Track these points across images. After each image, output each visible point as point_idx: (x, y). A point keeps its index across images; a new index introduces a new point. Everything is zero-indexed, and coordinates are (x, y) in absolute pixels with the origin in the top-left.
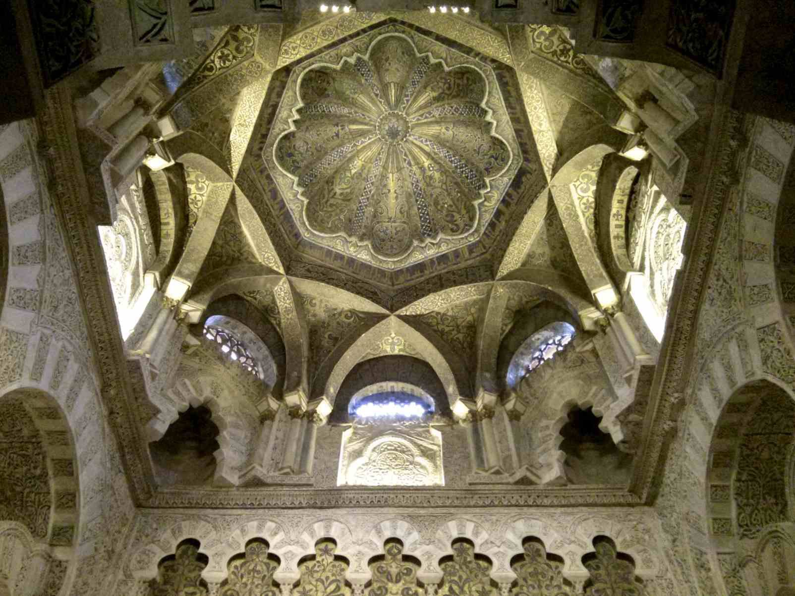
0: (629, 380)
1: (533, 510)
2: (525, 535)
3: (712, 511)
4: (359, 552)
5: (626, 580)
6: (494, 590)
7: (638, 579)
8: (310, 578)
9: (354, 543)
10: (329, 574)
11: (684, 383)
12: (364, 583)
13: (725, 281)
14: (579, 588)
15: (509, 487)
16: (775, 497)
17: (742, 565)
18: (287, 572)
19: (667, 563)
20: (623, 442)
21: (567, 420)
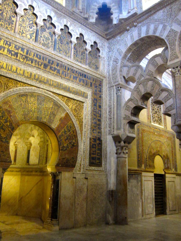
0: (129, 12)
1: (84, 27)
2: (81, 33)
3: (126, 52)
4: (41, 16)
5: (96, 55)
6: (70, 43)
7: (99, 56)
8: (25, 16)
9: (39, 11)
10: (31, 18)
11: (140, 22)
12: (41, 25)
13: (172, 10)
14: (88, 52)
15: (82, 18)
16: (137, 57)
17: (124, 66)
18: (20, 11)
19: (106, 55)
20: (115, 24)
21: (101, 7)
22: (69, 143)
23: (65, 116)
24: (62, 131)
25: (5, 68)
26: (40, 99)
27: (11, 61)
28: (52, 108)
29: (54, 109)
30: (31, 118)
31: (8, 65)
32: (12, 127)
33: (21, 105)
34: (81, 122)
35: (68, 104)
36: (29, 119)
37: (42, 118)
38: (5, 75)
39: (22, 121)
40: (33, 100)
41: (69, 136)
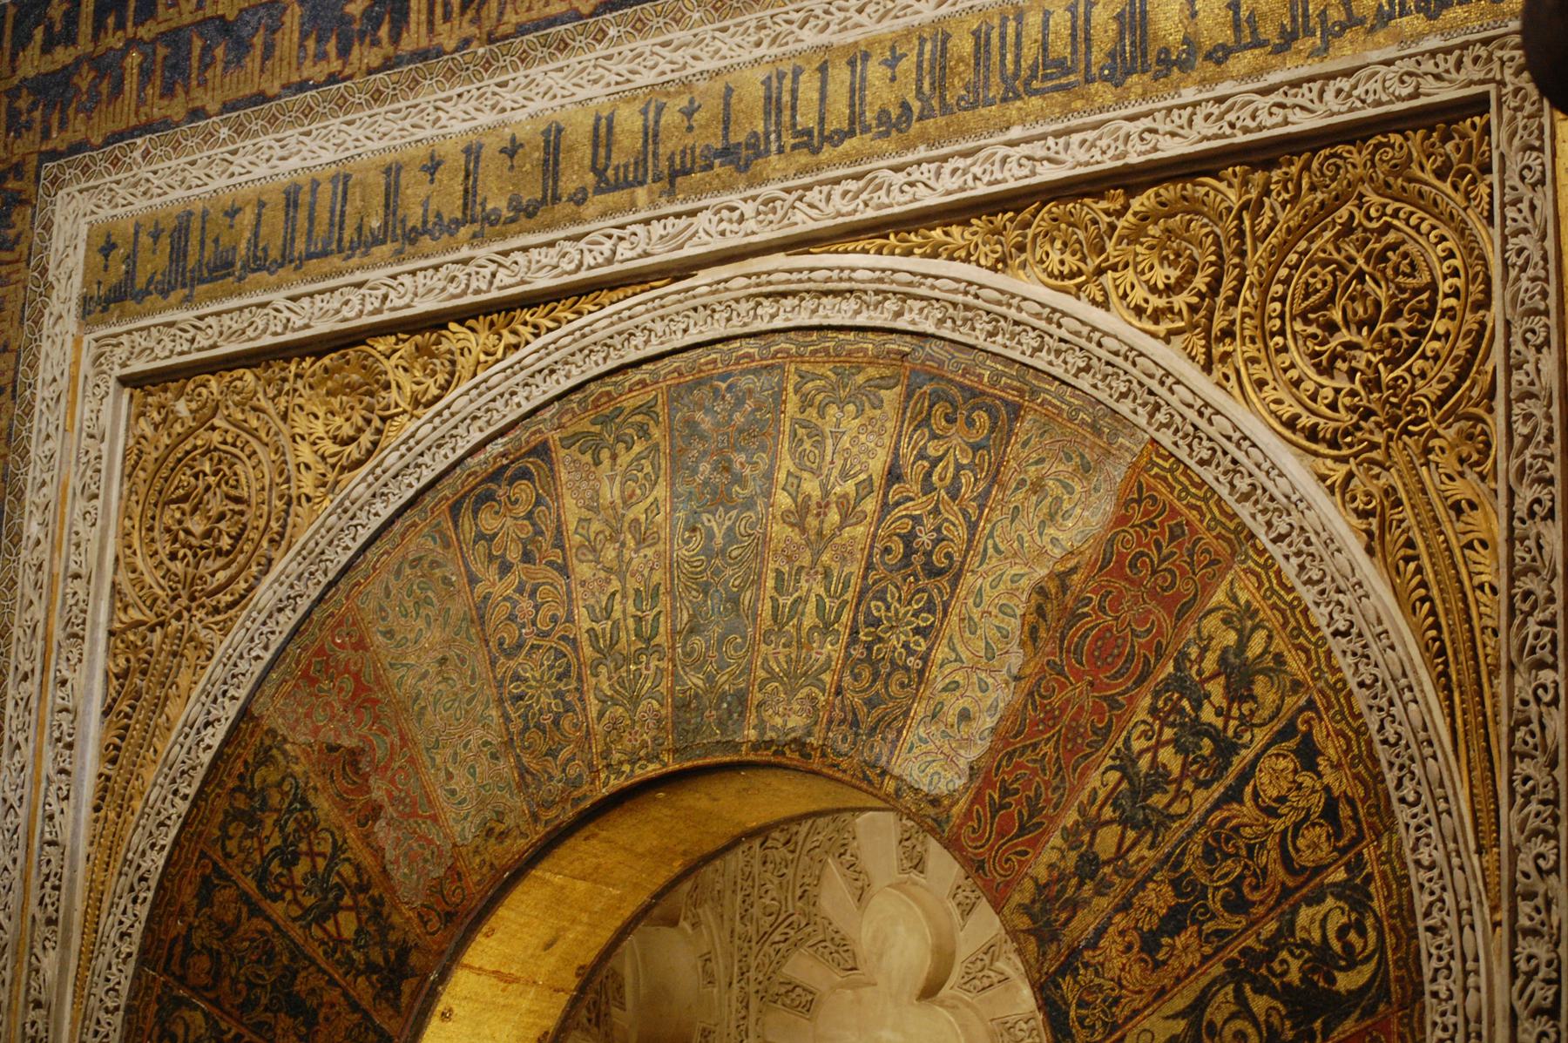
22: (1217, 969)
23: (1122, 520)
24: (1084, 796)
25: (274, 253)
26: (705, 422)
27: (335, 124)
28: (894, 475)
29: (928, 487)
30: (606, 754)
31: (305, 198)
32: (383, 943)
33: (482, 617)
34: (1457, 508)
35: (1169, 290)
36: (575, 783)
37: (741, 698)
38: (289, 336)
39: (491, 830)
40: (623, 484)
41: (1209, 854)
